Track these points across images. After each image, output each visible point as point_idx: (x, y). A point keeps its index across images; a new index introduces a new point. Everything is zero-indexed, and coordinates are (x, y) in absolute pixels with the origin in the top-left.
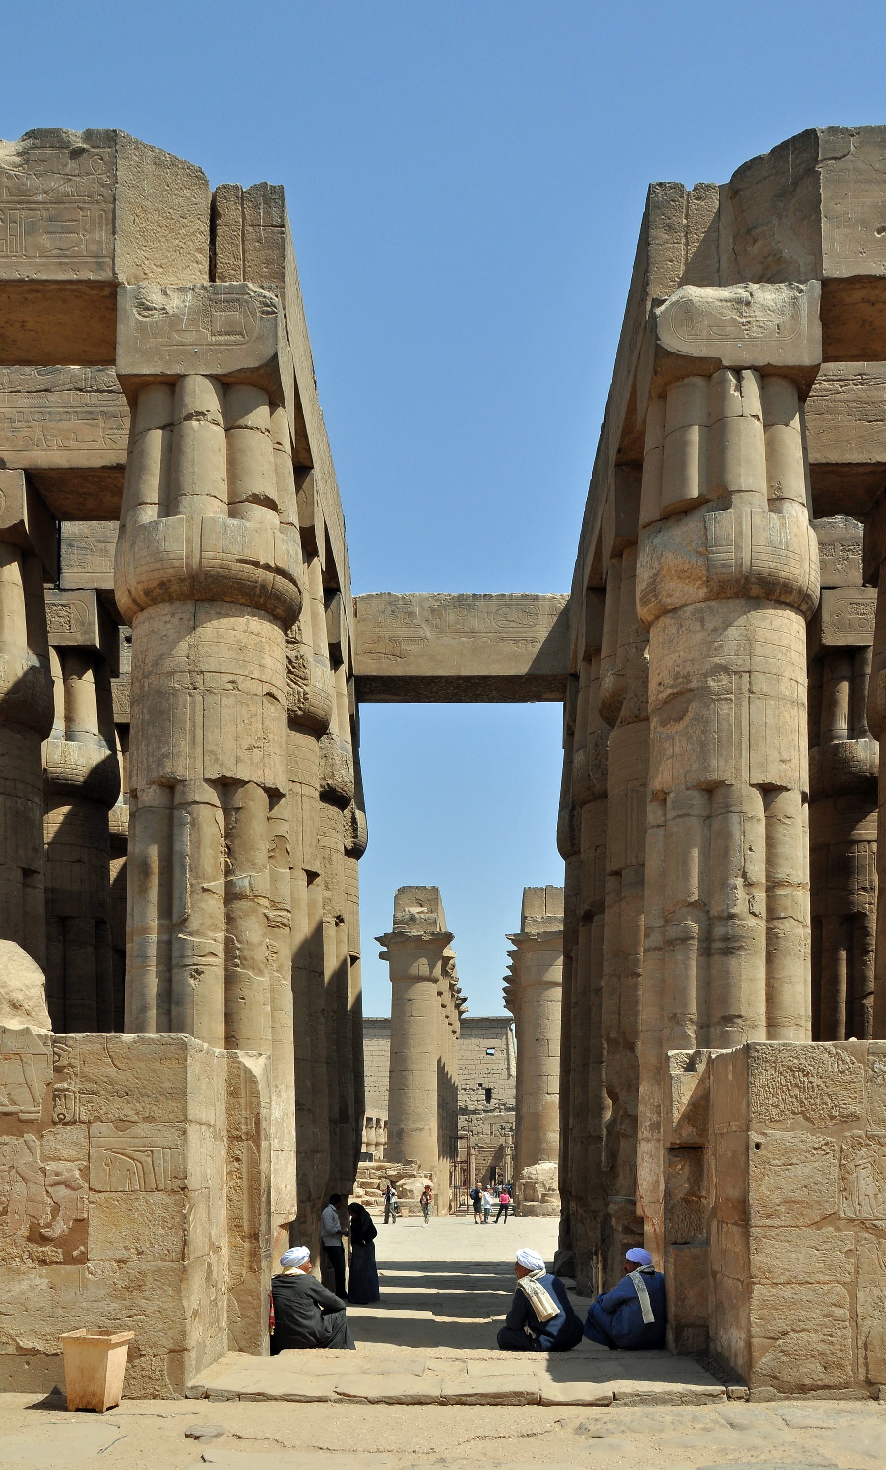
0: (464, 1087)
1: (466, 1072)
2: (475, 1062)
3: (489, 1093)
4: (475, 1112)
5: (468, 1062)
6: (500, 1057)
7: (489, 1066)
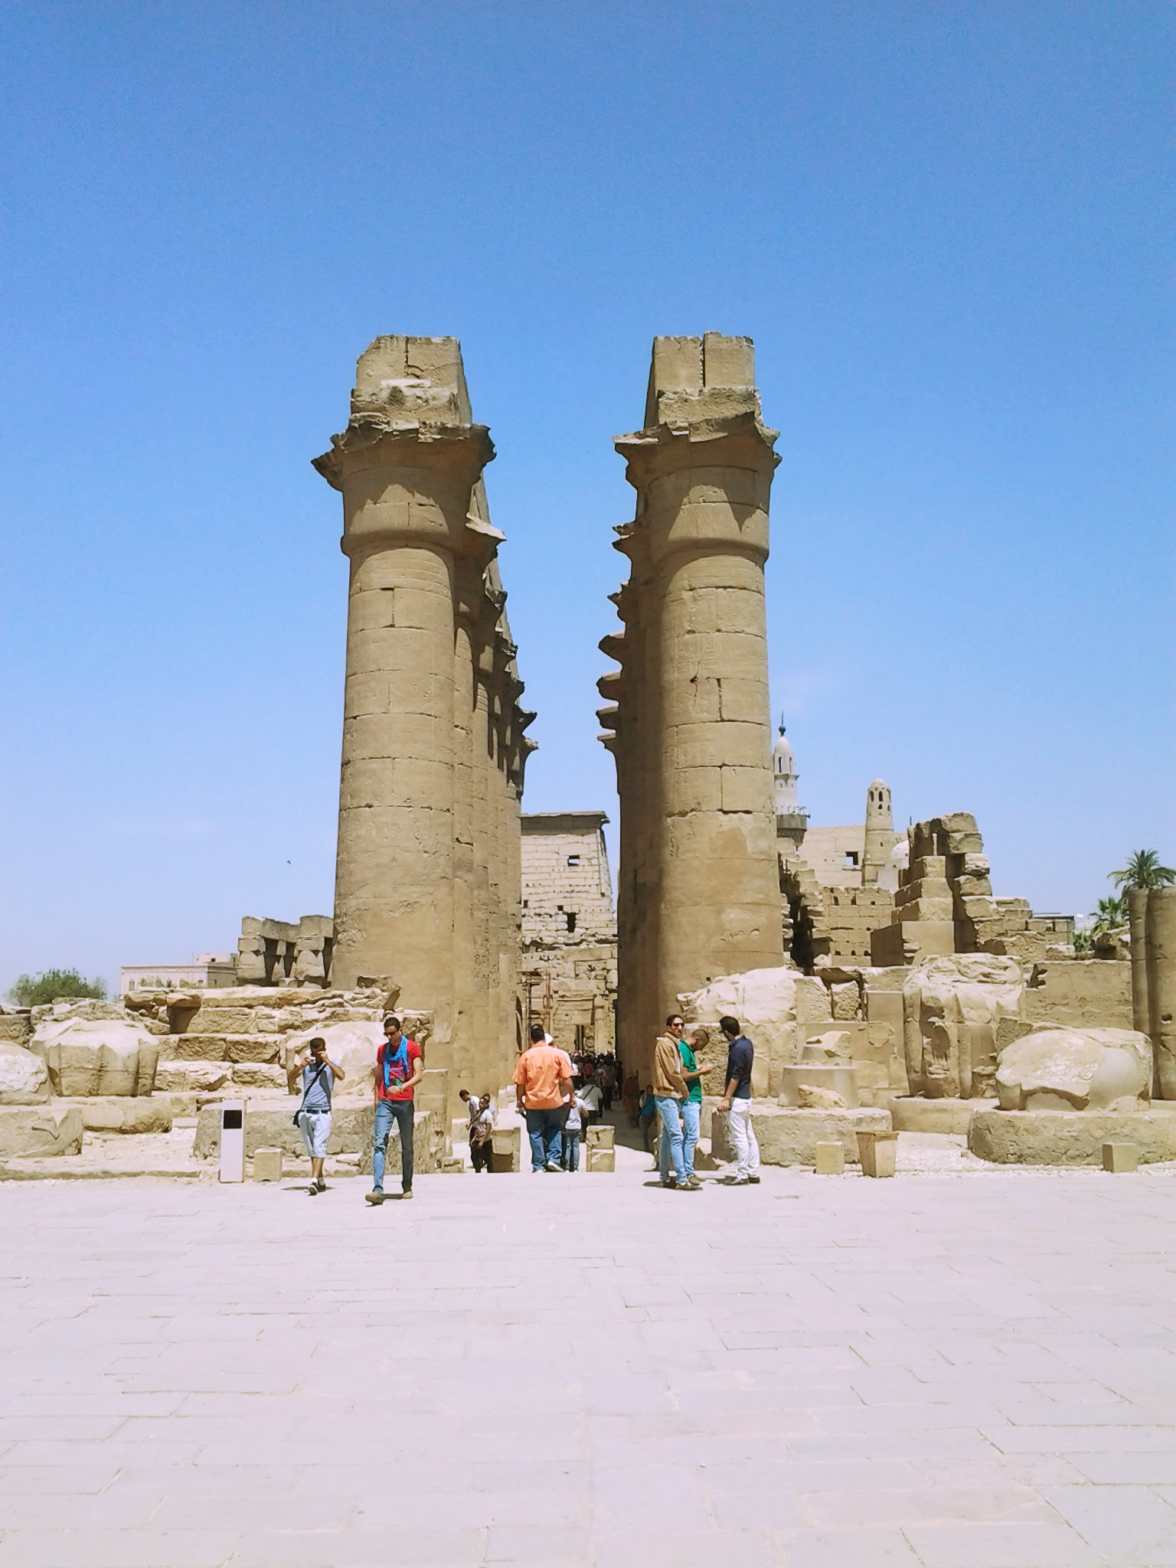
0: (538, 911)
1: (541, 890)
2: (554, 875)
3: (572, 920)
4: (551, 948)
5: (543, 876)
6: (587, 868)
7: (572, 882)
